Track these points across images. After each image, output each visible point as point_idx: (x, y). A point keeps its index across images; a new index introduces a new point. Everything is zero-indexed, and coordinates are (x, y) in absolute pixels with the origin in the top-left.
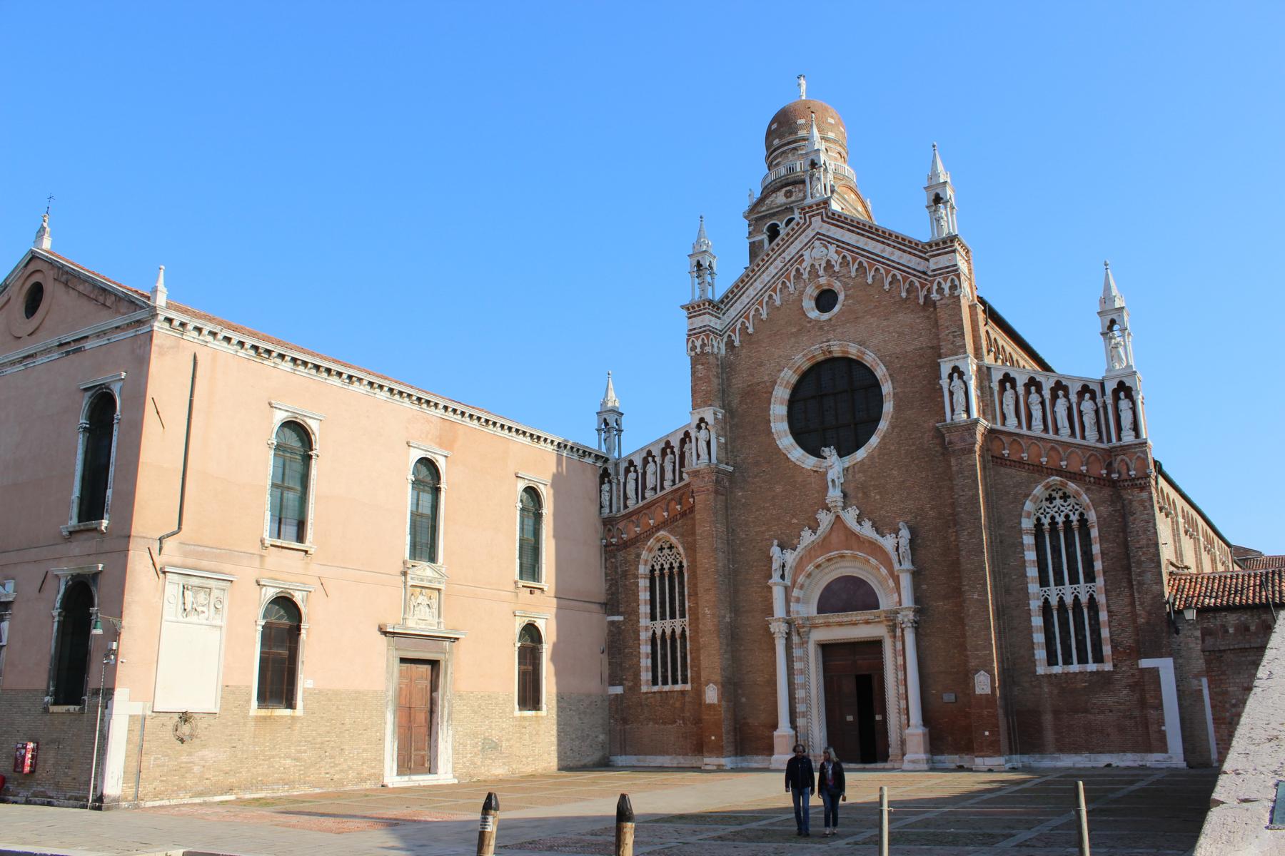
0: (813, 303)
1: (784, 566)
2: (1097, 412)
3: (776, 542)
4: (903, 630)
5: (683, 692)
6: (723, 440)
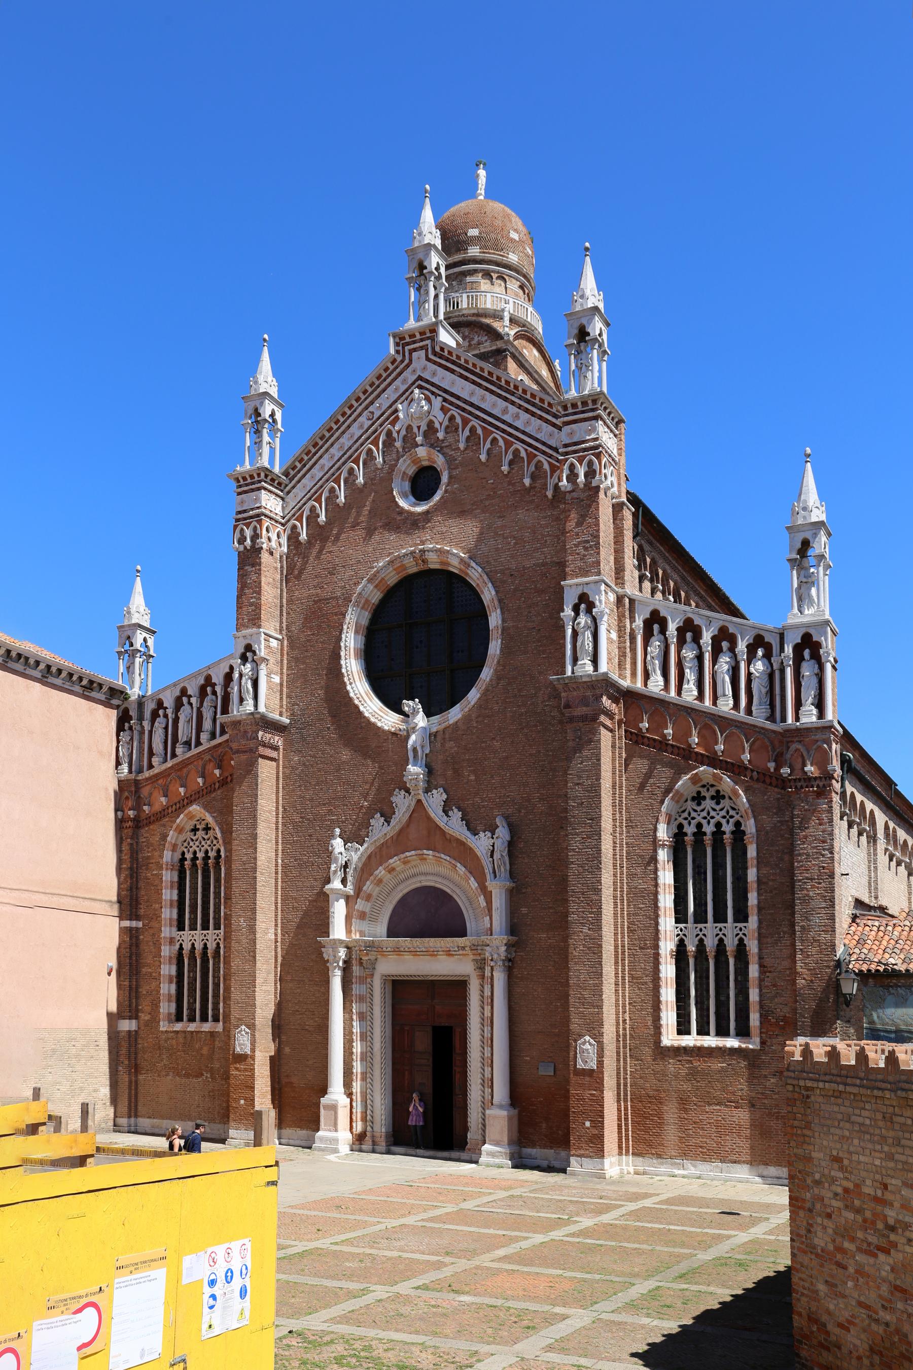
0: (407, 486)
2: (771, 676)
4: (492, 968)
6: (276, 679)
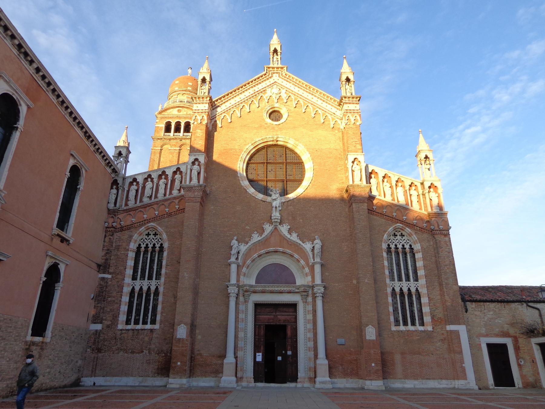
1: (238, 253)
3: (235, 238)
5: (152, 330)
